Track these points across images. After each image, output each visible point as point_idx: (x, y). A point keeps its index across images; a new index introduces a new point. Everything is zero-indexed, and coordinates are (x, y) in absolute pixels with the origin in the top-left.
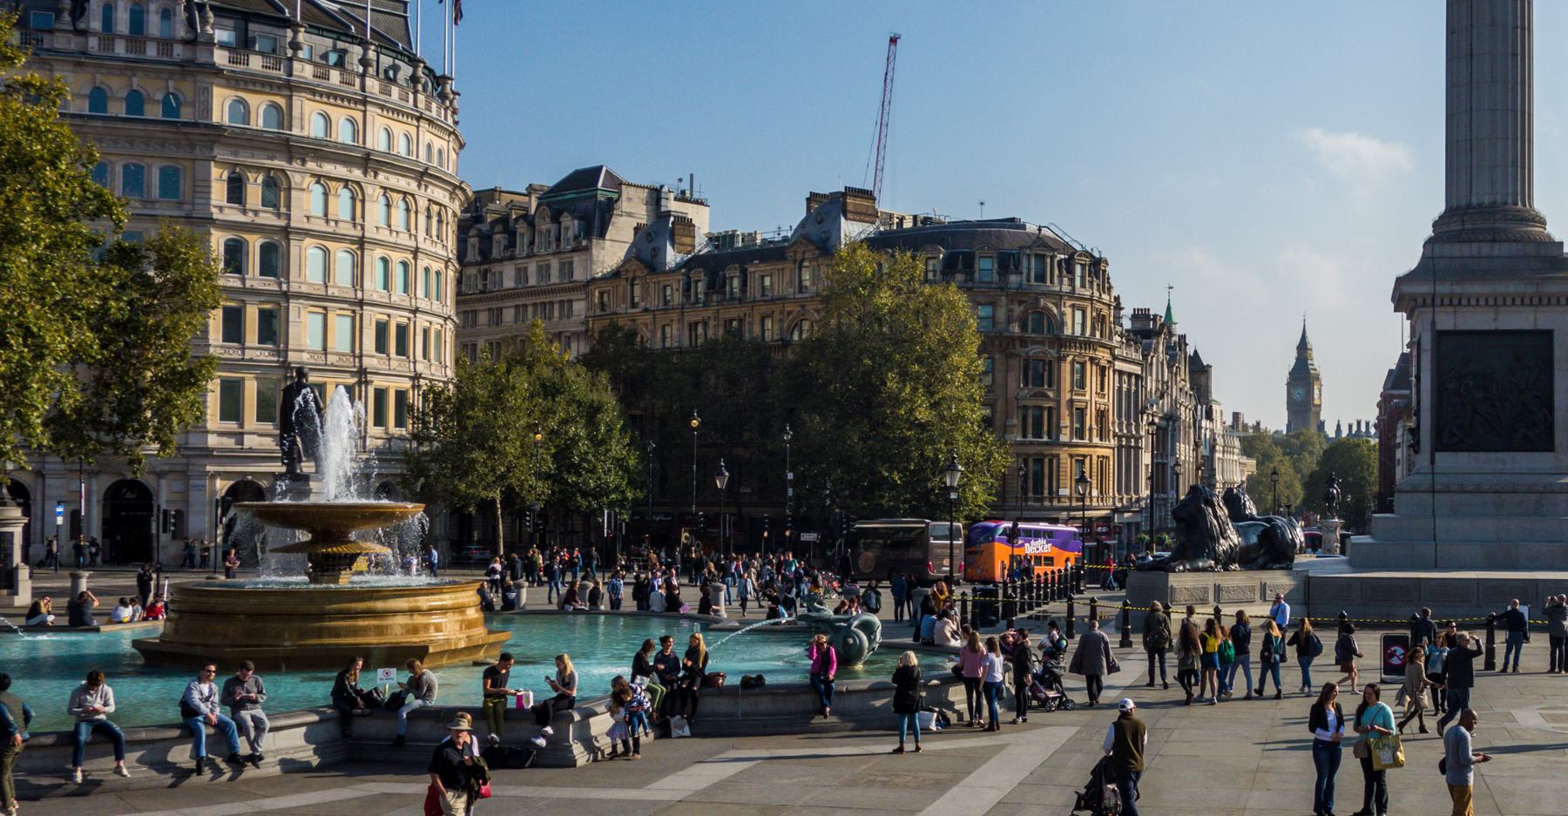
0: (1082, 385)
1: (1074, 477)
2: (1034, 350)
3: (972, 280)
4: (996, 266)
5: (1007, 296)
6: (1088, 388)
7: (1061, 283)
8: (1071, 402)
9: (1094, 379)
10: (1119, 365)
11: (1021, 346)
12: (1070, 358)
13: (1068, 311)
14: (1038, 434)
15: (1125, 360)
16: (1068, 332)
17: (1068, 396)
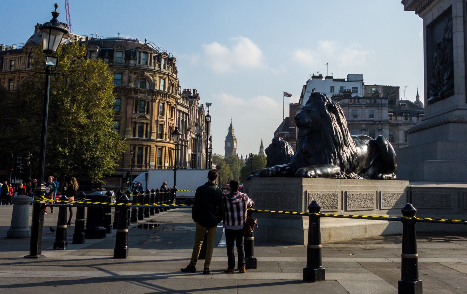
0: (163, 114)
1: (157, 157)
2: (140, 96)
3: (112, 62)
4: (124, 56)
5: (129, 70)
6: (165, 116)
7: (155, 66)
8: (157, 121)
9: (168, 111)
10: (179, 107)
11: (135, 94)
12: (157, 101)
13: (158, 79)
14: (141, 135)
15: (182, 105)
16: (157, 88)
17: (156, 118)
